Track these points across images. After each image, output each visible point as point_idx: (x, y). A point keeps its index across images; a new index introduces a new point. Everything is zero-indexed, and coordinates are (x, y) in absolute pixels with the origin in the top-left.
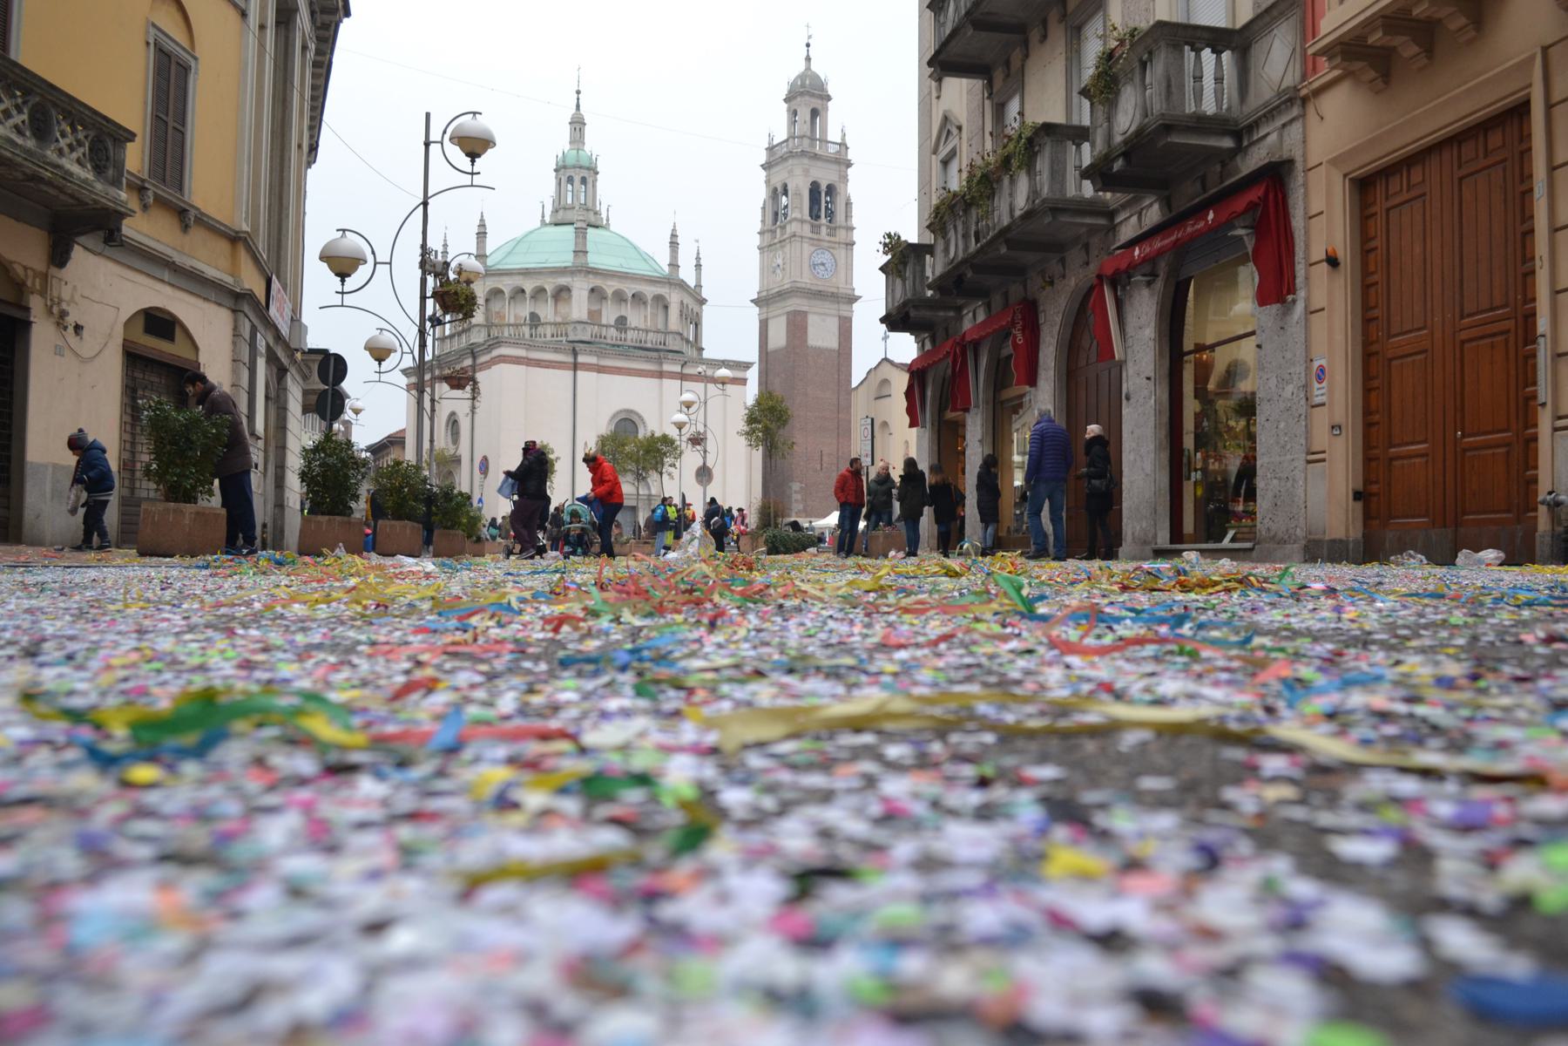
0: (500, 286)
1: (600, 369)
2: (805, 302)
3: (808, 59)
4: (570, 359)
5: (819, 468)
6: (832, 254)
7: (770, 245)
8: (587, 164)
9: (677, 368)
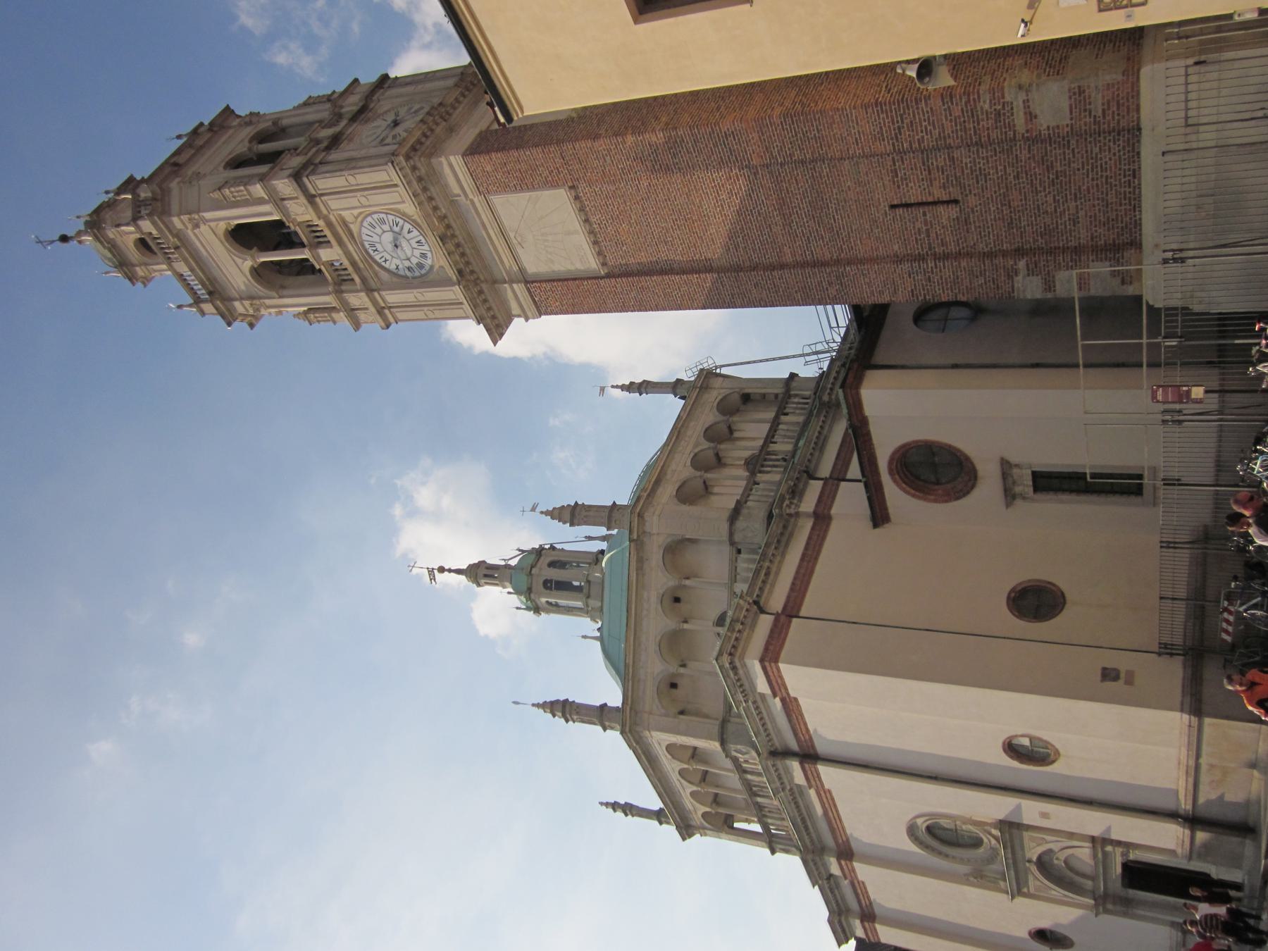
5: (953, 211)
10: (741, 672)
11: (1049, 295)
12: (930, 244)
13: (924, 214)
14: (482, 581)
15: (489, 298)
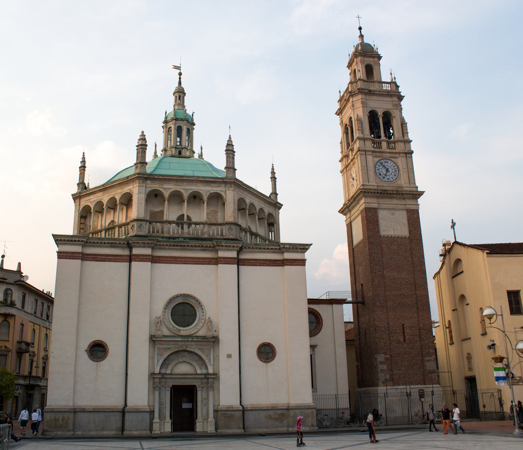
0: (89, 204)
1: (154, 260)
2: (374, 200)
3: (361, 36)
4: (126, 252)
5: (401, 338)
6: (394, 163)
7: (347, 166)
8: (182, 117)
9: (233, 254)
10: (300, 250)
11: (378, 363)
12: (392, 333)
13: (401, 333)
14: (177, 95)
15: (374, 194)
